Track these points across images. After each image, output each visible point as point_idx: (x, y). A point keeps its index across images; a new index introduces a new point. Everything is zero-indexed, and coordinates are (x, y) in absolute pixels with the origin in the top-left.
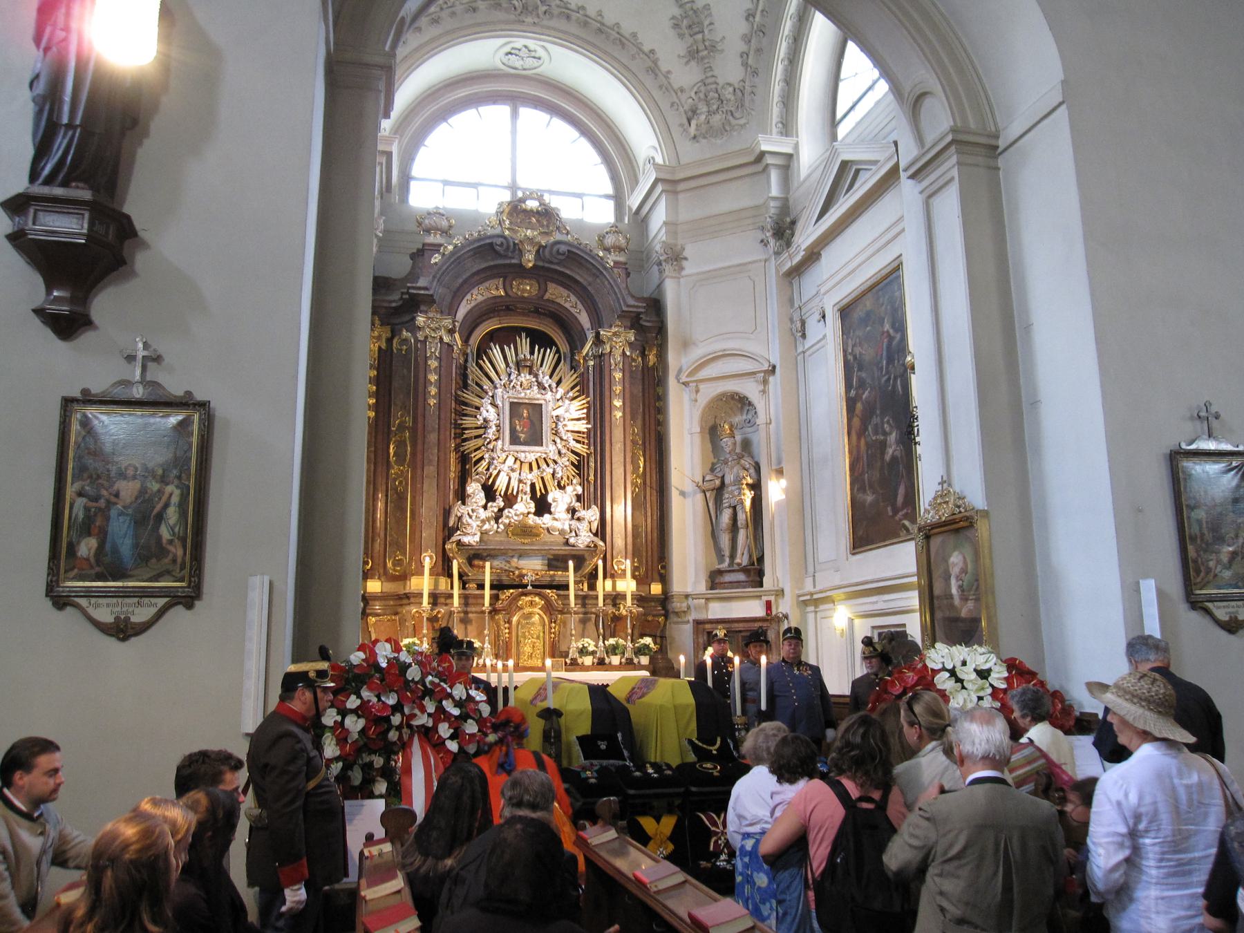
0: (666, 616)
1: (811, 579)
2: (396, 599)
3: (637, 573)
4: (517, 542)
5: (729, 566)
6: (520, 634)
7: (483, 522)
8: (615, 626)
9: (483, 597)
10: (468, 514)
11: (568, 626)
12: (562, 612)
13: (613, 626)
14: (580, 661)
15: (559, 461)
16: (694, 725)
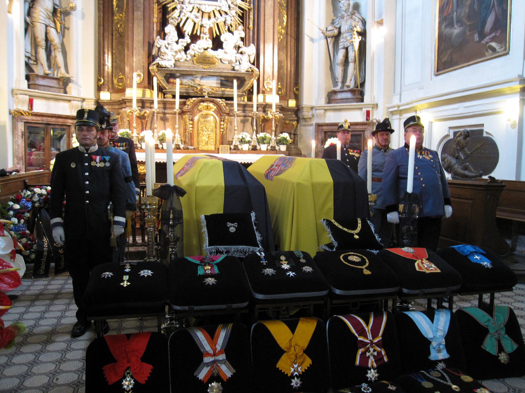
0: (298, 121)
1: (398, 96)
2: (119, 105)
3: (280, 93)
4: (200, 68)
5: (341, 88)
6: (200, 128)
7: (176, 52)
8: (264, 125)
9: (174, 103)
10: (165, 46)
11: (233, 125)
12: (228, 114)
13: (263, 125)
14: (240, 147)
15: (228, 12)
16: (330, 204)
